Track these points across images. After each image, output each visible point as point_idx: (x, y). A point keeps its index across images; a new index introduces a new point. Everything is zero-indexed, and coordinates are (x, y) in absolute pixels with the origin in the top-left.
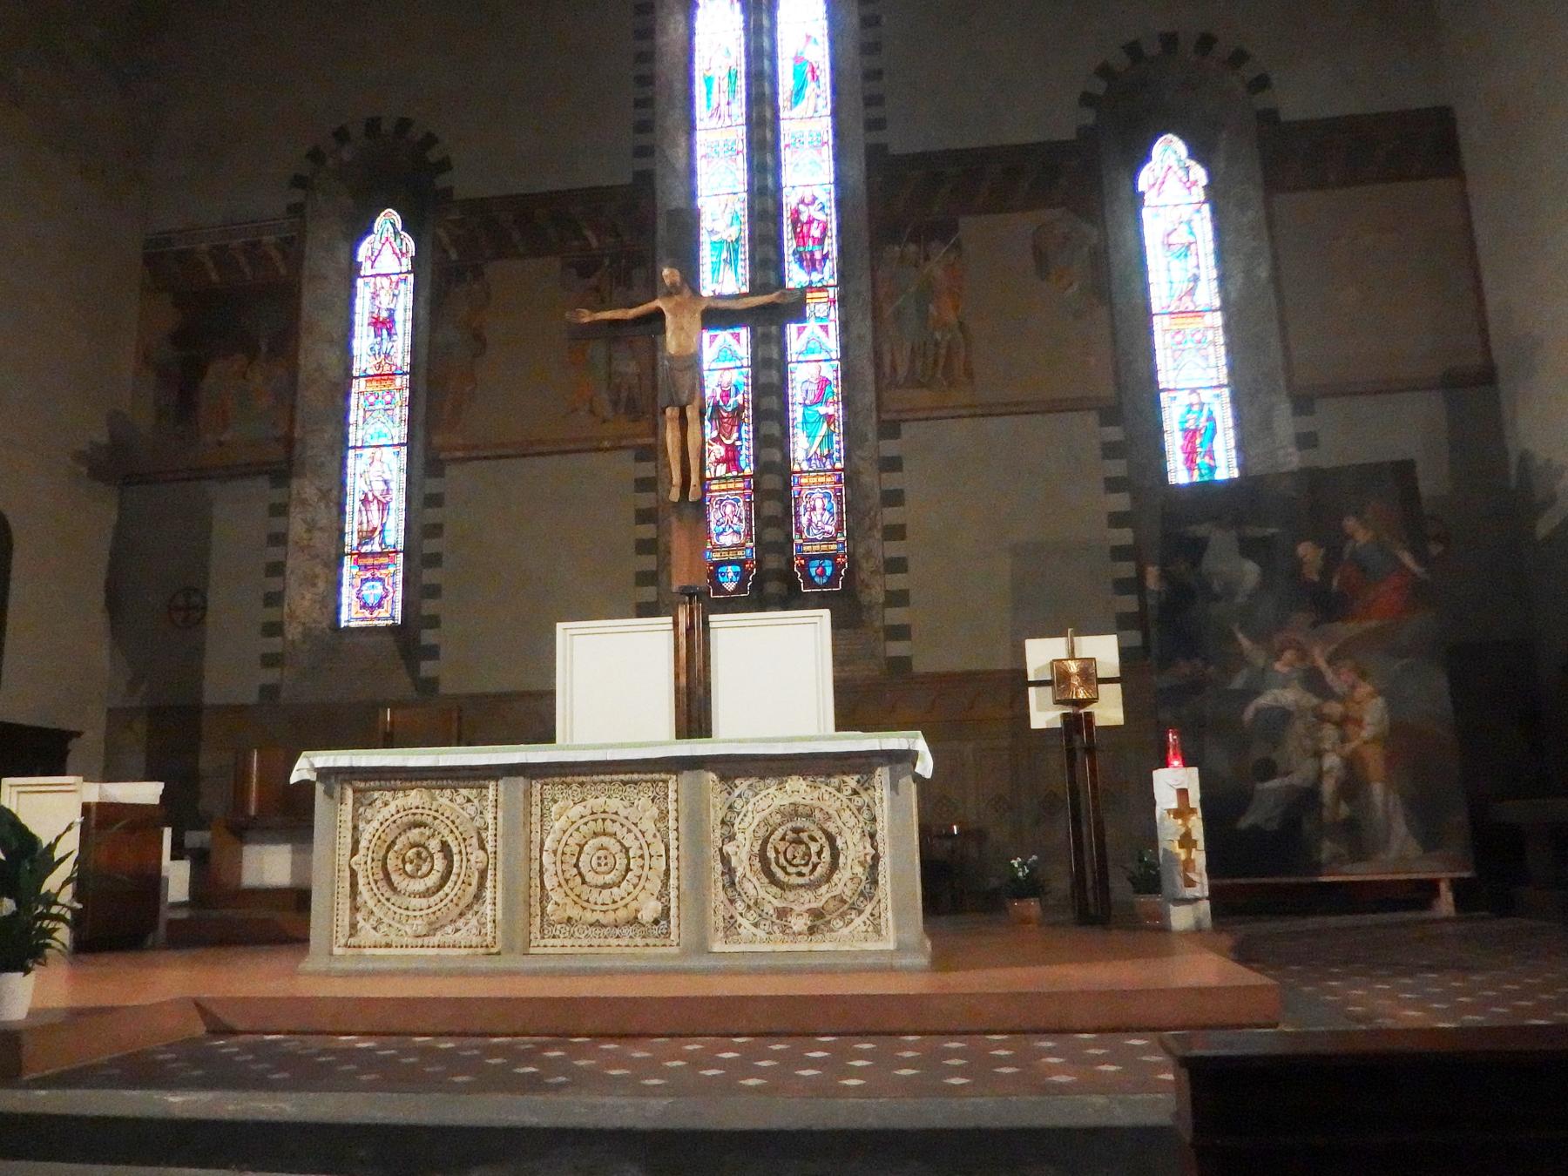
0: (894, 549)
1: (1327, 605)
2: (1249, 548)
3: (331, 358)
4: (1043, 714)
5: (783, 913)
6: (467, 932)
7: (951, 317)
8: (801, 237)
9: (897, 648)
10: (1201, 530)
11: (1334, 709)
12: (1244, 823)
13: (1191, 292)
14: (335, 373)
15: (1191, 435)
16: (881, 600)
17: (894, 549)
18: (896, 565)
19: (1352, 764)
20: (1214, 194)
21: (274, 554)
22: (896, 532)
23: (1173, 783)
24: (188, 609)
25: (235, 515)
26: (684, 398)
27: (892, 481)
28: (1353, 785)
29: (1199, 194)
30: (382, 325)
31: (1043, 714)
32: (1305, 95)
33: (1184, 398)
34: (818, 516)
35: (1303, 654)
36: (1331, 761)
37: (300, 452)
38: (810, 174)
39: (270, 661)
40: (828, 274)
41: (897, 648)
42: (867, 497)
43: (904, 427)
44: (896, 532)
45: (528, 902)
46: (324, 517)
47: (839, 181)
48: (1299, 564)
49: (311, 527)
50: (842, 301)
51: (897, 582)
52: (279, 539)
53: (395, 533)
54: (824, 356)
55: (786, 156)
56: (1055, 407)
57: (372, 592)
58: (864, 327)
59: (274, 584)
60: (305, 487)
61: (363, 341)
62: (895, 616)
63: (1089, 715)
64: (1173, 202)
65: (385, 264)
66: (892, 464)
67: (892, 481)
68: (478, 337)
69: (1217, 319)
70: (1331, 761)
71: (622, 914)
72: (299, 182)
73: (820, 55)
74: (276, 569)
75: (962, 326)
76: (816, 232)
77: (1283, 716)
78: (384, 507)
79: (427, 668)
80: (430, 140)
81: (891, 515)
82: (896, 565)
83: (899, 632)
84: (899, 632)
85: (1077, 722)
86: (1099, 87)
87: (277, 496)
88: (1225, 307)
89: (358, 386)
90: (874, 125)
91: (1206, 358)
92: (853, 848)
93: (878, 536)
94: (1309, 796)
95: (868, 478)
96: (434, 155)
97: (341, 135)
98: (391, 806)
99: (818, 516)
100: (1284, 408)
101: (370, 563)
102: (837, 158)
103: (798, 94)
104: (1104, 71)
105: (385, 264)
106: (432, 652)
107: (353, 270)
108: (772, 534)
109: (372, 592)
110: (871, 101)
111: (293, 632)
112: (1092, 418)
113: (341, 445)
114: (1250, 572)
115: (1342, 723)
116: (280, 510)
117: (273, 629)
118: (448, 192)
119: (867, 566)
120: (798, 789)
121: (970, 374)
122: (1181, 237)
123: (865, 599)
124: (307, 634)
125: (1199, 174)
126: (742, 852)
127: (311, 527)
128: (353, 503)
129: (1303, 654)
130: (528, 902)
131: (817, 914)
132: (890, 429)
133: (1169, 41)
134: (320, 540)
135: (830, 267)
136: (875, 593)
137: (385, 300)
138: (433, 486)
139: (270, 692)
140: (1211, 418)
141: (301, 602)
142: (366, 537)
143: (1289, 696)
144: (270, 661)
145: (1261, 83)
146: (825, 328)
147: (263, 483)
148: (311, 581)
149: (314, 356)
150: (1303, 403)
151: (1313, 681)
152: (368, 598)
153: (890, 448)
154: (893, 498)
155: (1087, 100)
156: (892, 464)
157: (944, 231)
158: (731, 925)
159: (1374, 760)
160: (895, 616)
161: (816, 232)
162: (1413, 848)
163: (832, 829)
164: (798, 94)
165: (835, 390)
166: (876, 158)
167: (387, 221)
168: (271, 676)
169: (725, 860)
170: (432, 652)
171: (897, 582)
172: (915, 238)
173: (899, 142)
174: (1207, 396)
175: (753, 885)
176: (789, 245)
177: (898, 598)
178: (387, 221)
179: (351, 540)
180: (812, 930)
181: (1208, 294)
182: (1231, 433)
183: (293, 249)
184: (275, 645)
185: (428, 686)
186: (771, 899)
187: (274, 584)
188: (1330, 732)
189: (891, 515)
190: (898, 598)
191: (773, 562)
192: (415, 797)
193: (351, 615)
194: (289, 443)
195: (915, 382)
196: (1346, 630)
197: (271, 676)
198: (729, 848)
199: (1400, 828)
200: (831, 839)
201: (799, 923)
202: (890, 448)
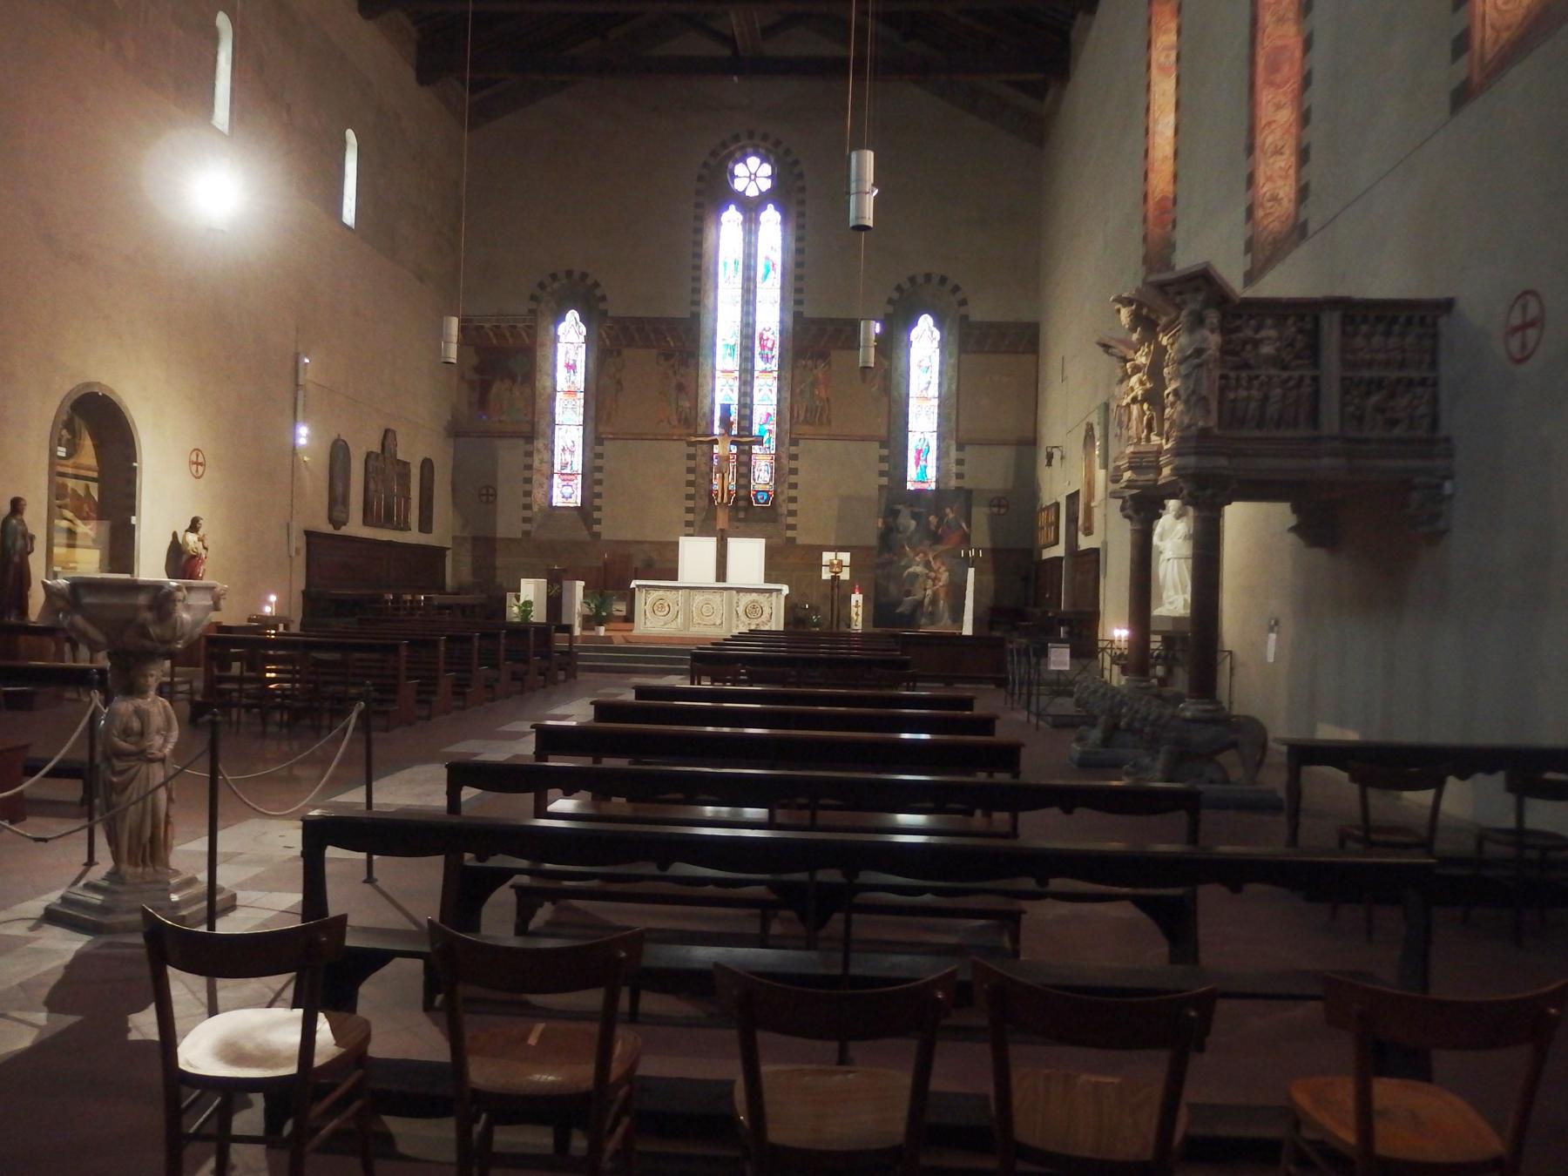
0: (793, 493)
1: (936, 538)
2: (915, 516)
3: (548, 383)
4: (826, 575)
6: (673, 625)
7: (823, 395)
8: (763, 347)
9: (790, 534)
10: (899, 507)
11: (932, 575)
12: (899, 610)
14: (549, 390)
15: (919, 452)
17: (793, 493)
18: (793, 500)
19: (935, 594)
20: (943, 345)
21: (527, 474)
22: (794, 486)
23: (857, 598)
24: (488, 495)
25: (508, 455)
27: (793, 464)
28: (934, 602)
29: (936, 344)
30: (571, 367)
31: (826, 575)
32: (982, 311)
33: (918, 436)
34: (762, 474)
35: (926, 554)
36: (929, 592)
37: (533, 429)
38: (770, 317)
39: (526, 520)
40: (774, 365)
41: (790, 534)
44: (794, 486)
45: (688, 619)
46: (546, 457)
47: (781, 322)
48: (928, 523)
49: (542, 461)
50: (779, 378)
51: (792, 506)
52: (529, 467)
53: (577, 466)
55: (758, 306)
56: (863, 439)
57: (567, 491)
58: (787, 395)
59: (527, 487)
60: (539, 444)
61: (562, 374)
62: (791, 520)
64: (925, 343)
65: (570, 338)
66: (794, 457)
67: (793, 464)
68: (619, 382)
69: (936, 402)
70: (929, 592)
72: (533, 298)
73: (777, 257)
74: (528, 481)
76: (769, 344)
77: (916, 575)
78: (572, 452)
79: (596, 528)
80: (596, 285)
81: (793, 479)
82: (793, 500)
83: (792, 527)
84: (792, 527)
86: (896, 295)
87: (529, 447)
88: (939, 397)
89: (559, 396)
90: (798, 302)
92: (767, 611)
94: (920, 603)
95: (784, 461)
96: (599, 293)
97: (554, 277)
98: (655, 595)
99: (762, 474)
100: (953, 448)
101: (567, 477)
102: (782, 310)
103: (765, 277)
104: (899, 288)
105: (570, 338)
106: (599, 521)
107: (556, 339)
108: (742, 481)
109: (567, 491)
110: (798, 291)
111: (535, 508)
112: (877, 445)
113: (553, 423)
114: (913, 523)
115: (934, 580)
116: (529, 454)
117: (528, 507)
118: (606, 311)
119: (781, 498)
120: (755, 596)
121: (829, 422)
122: (925, 363)
124: (541, 510)
125: (937, 334)
126: (741, 610)
127: (542, 461)
128: (558, 451)
129: (926, 554)
130: (688, 619)
132: (794, 442)
133: (928, 277)
134: (545, 467)
135: (775, 361)
136: (784, 510)
137: (572, 356)
138: (599, 449)
139: (526, 533)
141: (538, 494)
142: (564, 466)
143: (918, 569)
144: (526, 520)
145: (963, 303)
147: (521, 442)
148: (541, 485)
149: (543, 382)
150: (960, 447)
151: (927, 565)
152: (566, 493)
153: (793, 450)
154: (794, 471)
155: (890, 301)
156: (794, 457)
157: (823, 356)
159: (942, 594)
160: (791, 520)
161: (769, 344)
162: (949, 622)
164: (765, 277)
165: (774, 418)
166: (797, 316)
167: (572, 316)
168: (527, 527)
170: (599, 521)
171: (792, 506)
172: (811, 358)
173: (809, 312)
174: (927, 436)
175: (743, 618)
176: (757, 350)
177: (792, 513)
178: (572, 316)
179: (557, 468)
181: (934, 391)
183: (532, 331)
184: (528, 514)
185: (597, 535)
187: (527, 487)
188: (930, 582)
189: (793, 479)
190: (792, 513)
191: (742, 492)
192: (661, 592)
193: (557, 501)
194: (533, 424)
195: (806, 422)
196: (941, 548)
197: (527, 527)
199: (946, 615)
202: (793, 450)
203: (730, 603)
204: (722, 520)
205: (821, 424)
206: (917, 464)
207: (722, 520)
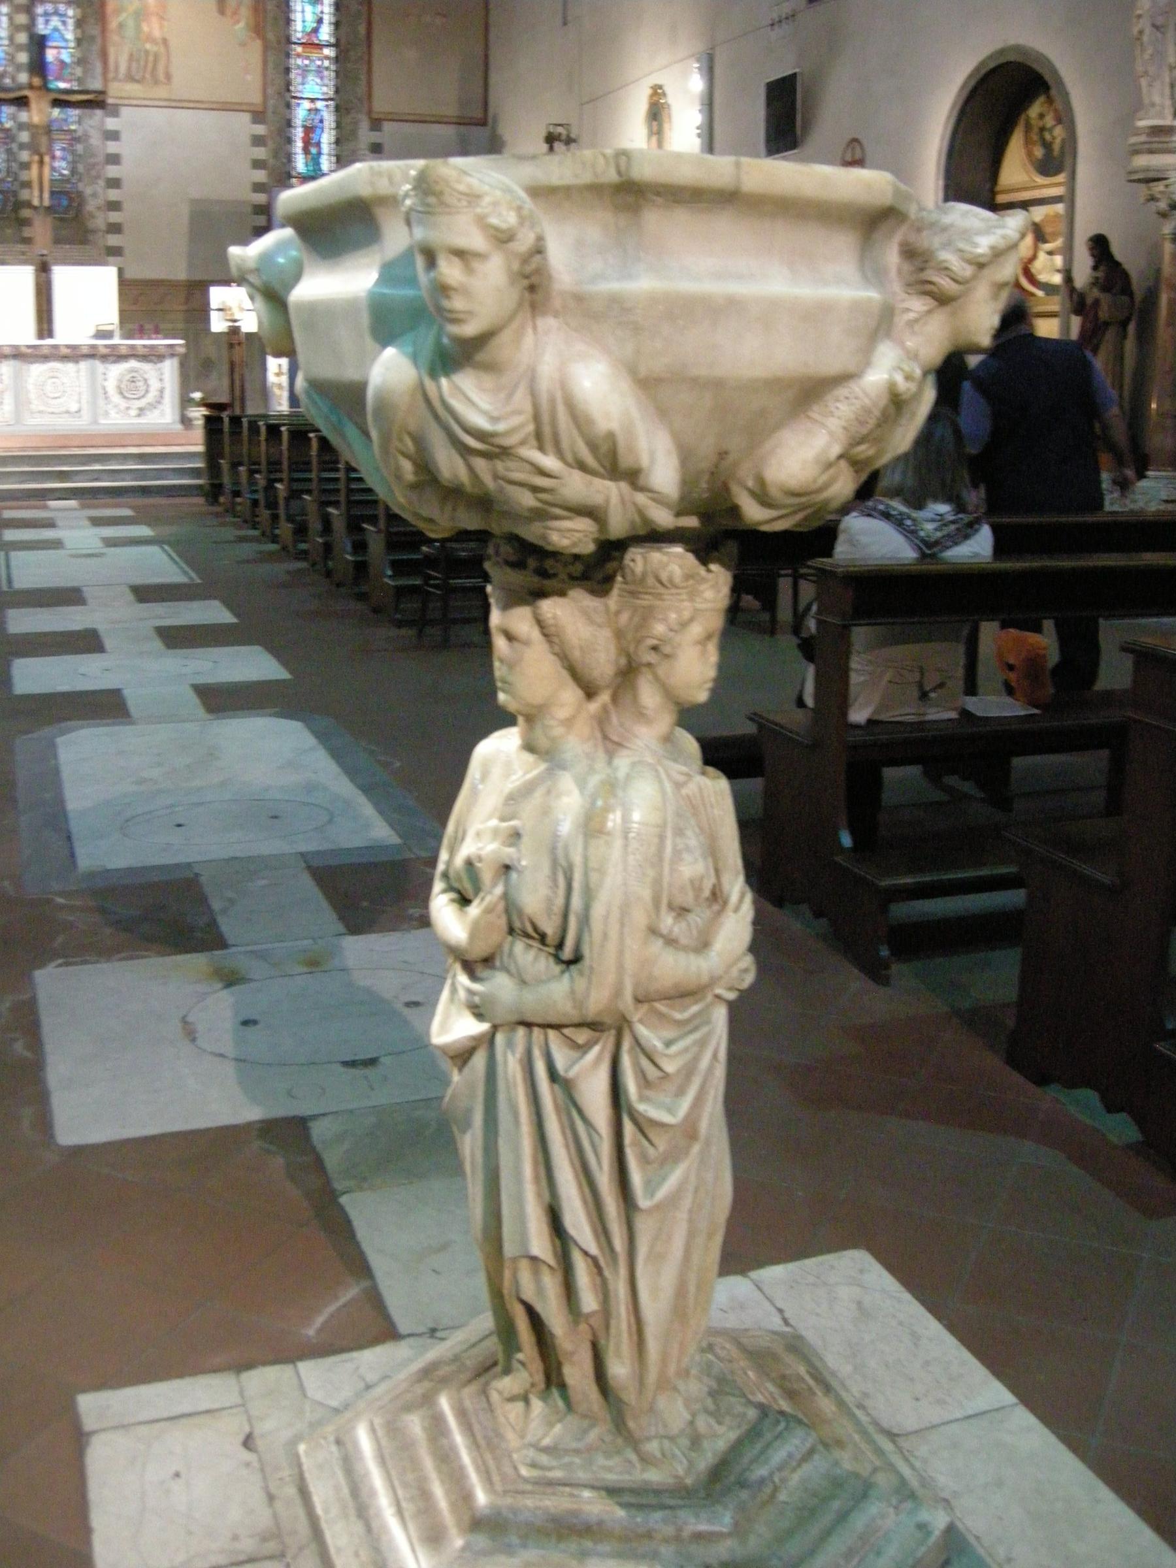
4: (218, 324)
5: (128, 408)
7: (157, 34)
13: (315, 31)
15: (309, 130)
16: (103, 227)
17: (113, 195)
22: (115, 183)
26: (43, 149)
33: (306, 105)
42: (93, 155)
43: (125, 111)
51: (114, 217)
54: (62, 44)
62: (113, 240)
63: (238, 328)
71: (64, 409)
75: (165, 41)
82: (115, 206)
85: (234, 331)
91: (322, 78)
92: (155, 385)
93: (101, 183)
112: (247, 117)
121: (168, 77)
123: (91, 224)
126: (111, 385)
131: (141, 409)
140: (321, 121)
146: (64, 23)
158: (107, 413)
160: (113, 240)
163: (146, 376)
169: (104, 388)
171: (114, 217)
174: (320, 105)
175: (116, 399)
177: (115, 228)
180: (139, 415)
182: (333, 132)
186: (123, 404)
190: (115, 228)
198: (106, 384)
200: (146, 380)
201: (133, 412)
203: (93, 373)
204: (41, 230)
205: (156, 82)
206: (306, 150)
207: (41, 230)
